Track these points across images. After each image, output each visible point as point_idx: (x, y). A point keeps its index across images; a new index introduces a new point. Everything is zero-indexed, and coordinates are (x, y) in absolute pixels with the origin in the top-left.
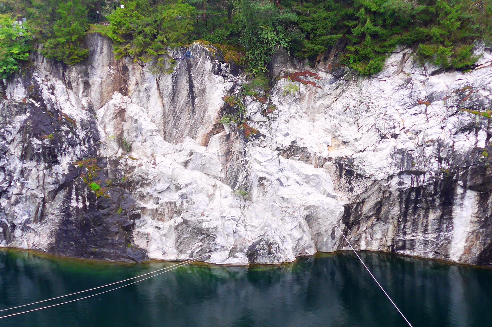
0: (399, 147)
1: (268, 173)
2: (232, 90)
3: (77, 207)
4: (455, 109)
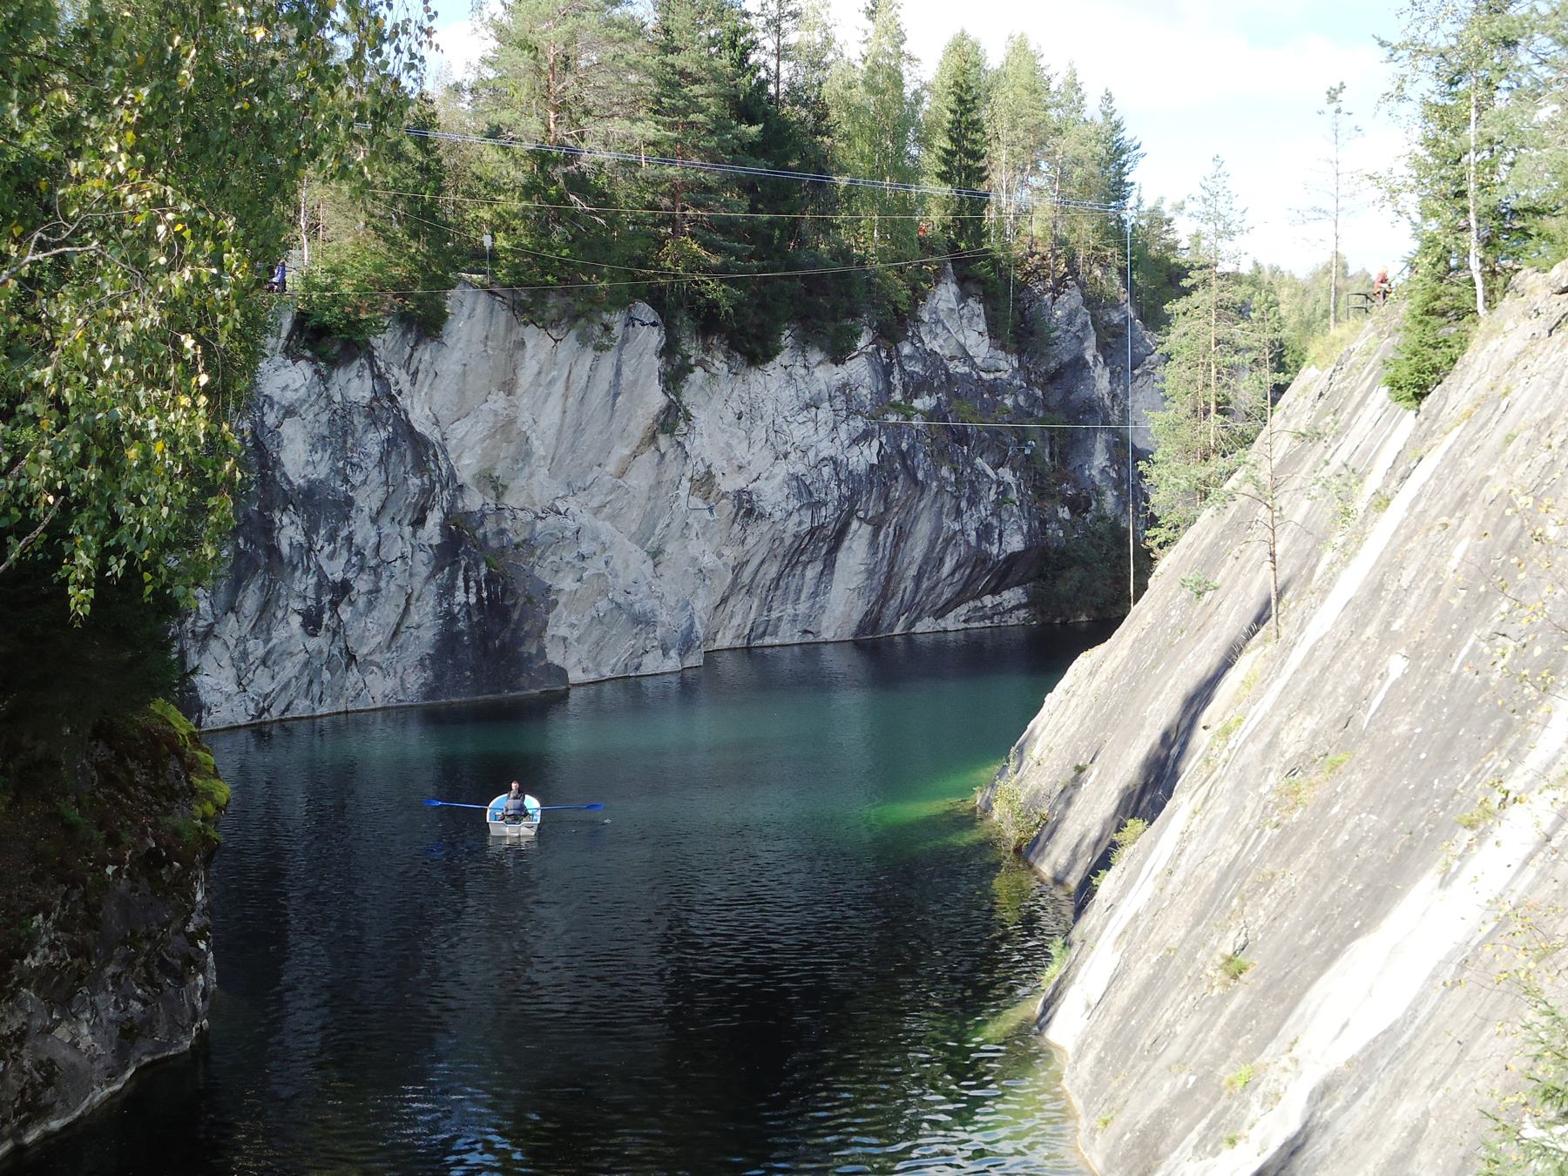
3: (467, 603)
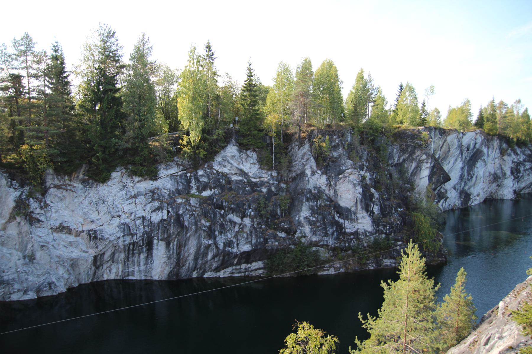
0: (122, 221)
1: (46, 243)
2: (20, 196)
4: (150, 200)
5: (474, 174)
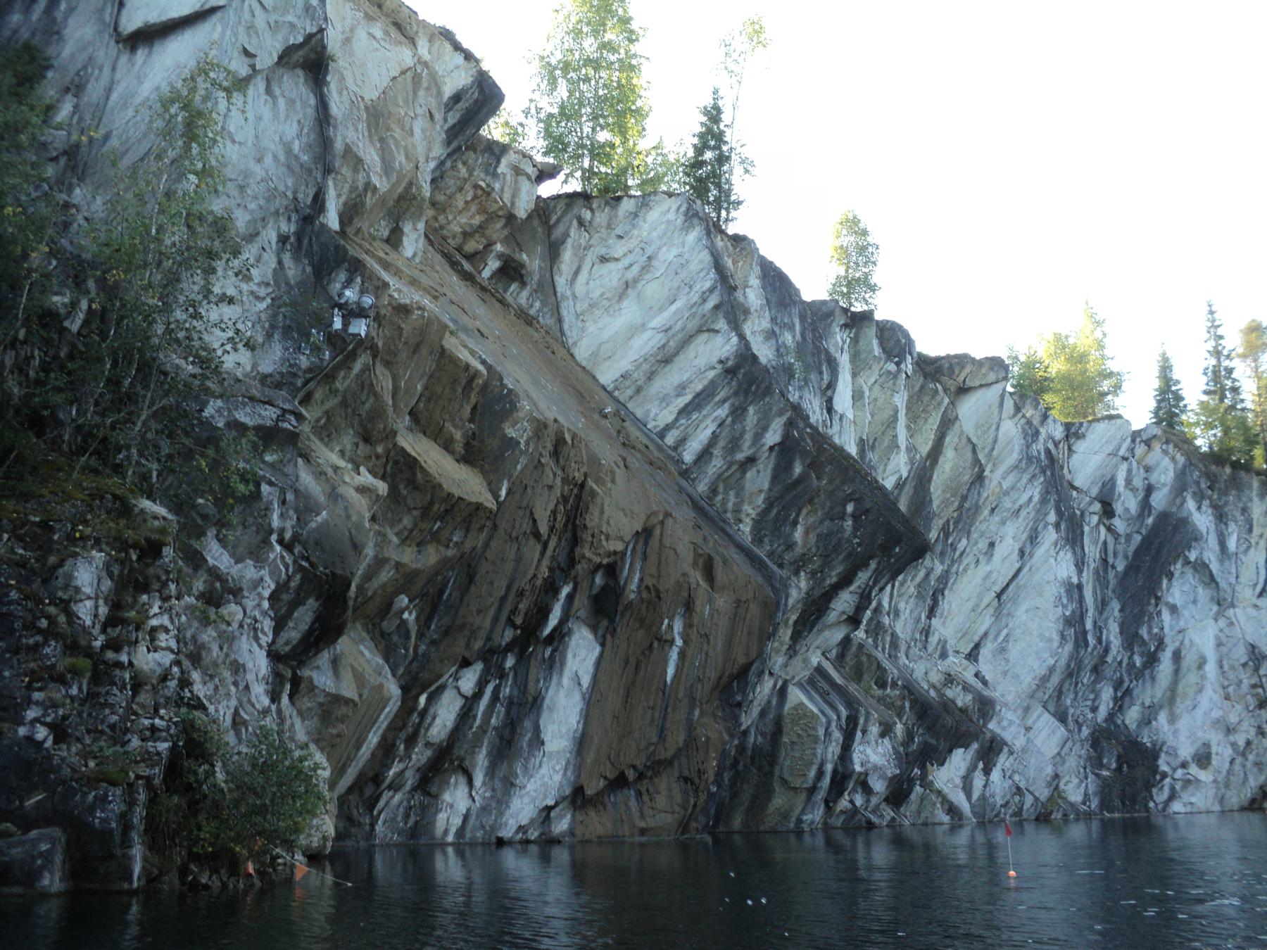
5: (1161, 644)
